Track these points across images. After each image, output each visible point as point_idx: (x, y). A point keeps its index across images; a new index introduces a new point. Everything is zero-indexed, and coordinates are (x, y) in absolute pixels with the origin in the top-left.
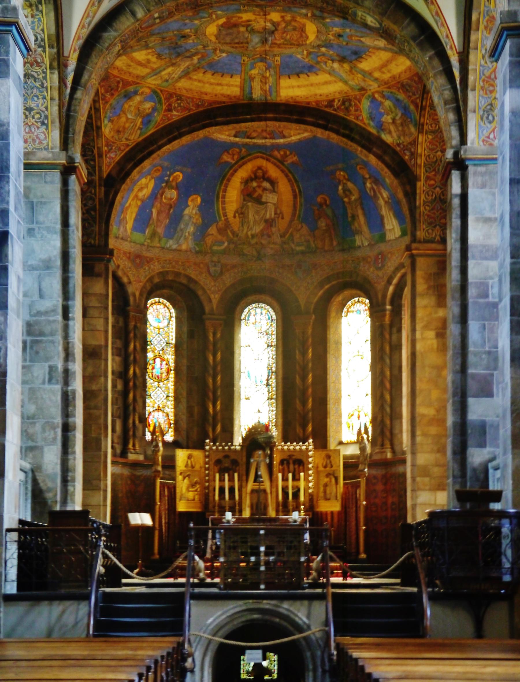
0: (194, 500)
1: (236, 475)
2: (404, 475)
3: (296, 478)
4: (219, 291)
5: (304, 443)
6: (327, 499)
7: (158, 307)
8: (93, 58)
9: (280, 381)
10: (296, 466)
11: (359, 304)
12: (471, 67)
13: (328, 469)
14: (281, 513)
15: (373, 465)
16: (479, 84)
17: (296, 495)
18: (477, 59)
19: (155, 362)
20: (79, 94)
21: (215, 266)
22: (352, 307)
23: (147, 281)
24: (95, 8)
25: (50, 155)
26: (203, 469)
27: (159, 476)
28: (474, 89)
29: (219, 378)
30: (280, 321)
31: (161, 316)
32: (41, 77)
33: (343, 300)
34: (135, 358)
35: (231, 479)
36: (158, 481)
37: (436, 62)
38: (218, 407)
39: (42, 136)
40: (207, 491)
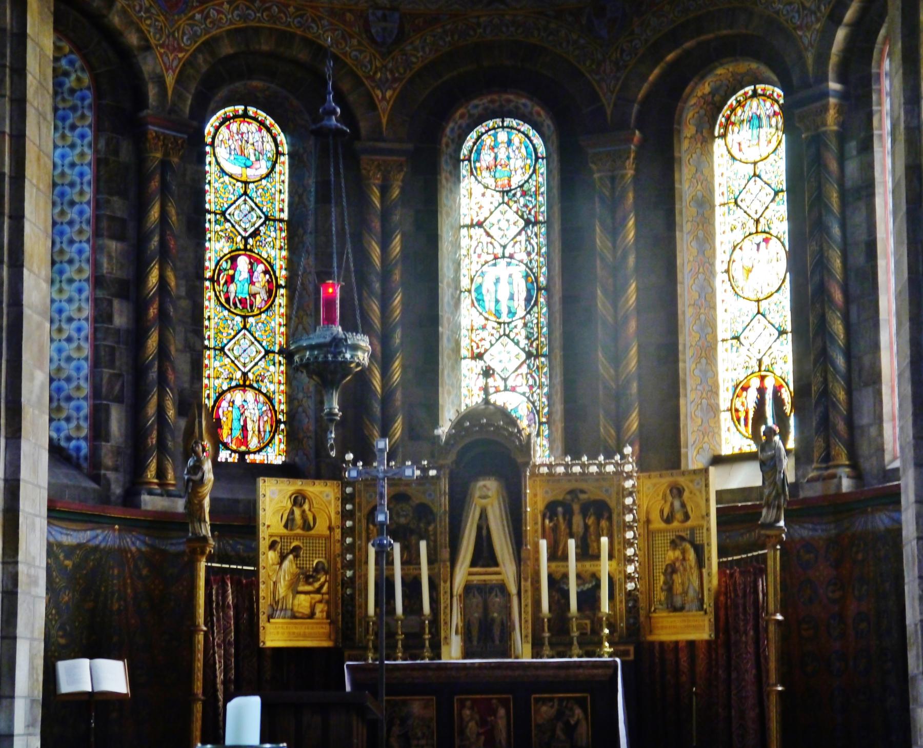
0: (312, 615)
1: (423, 545)
2: (896, 534)
3: (587, 553)
4: (395, 80)
5: (609, 456)
6: (675, 609)
7: (244, 127)
9: (557, 307)
10: (591, 521)
11: (755, 102)
13: (675, 524)
14: (547, 650)
15: (801, 510)
17: (589, 599)
19: (234, 266)
21: (384, 18)
22: (739, 111)
23: (198, 50)
26: (338, 534)
27: (203, 553)
29: (398, 300)
30: (555, 157)
31: (250, 150)
33: (713, 93)
34: (163, 243)
35: (411, 559)
36: (203, 564)
38: (397, 376)
40: (349, 591)
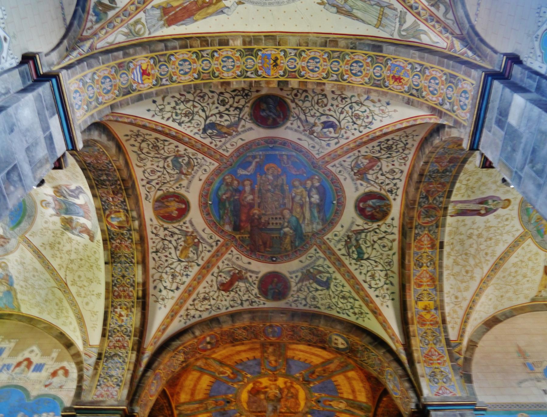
8: (164, 354)
12: (414, 348)
16: (422, 359)
18: (416, 343)
20: (149, 374)
24: (169, 320)
25: (116, 403)
28: (419, 363)
32: (124, 356)
37: (388, 355)
39: (115, 393)
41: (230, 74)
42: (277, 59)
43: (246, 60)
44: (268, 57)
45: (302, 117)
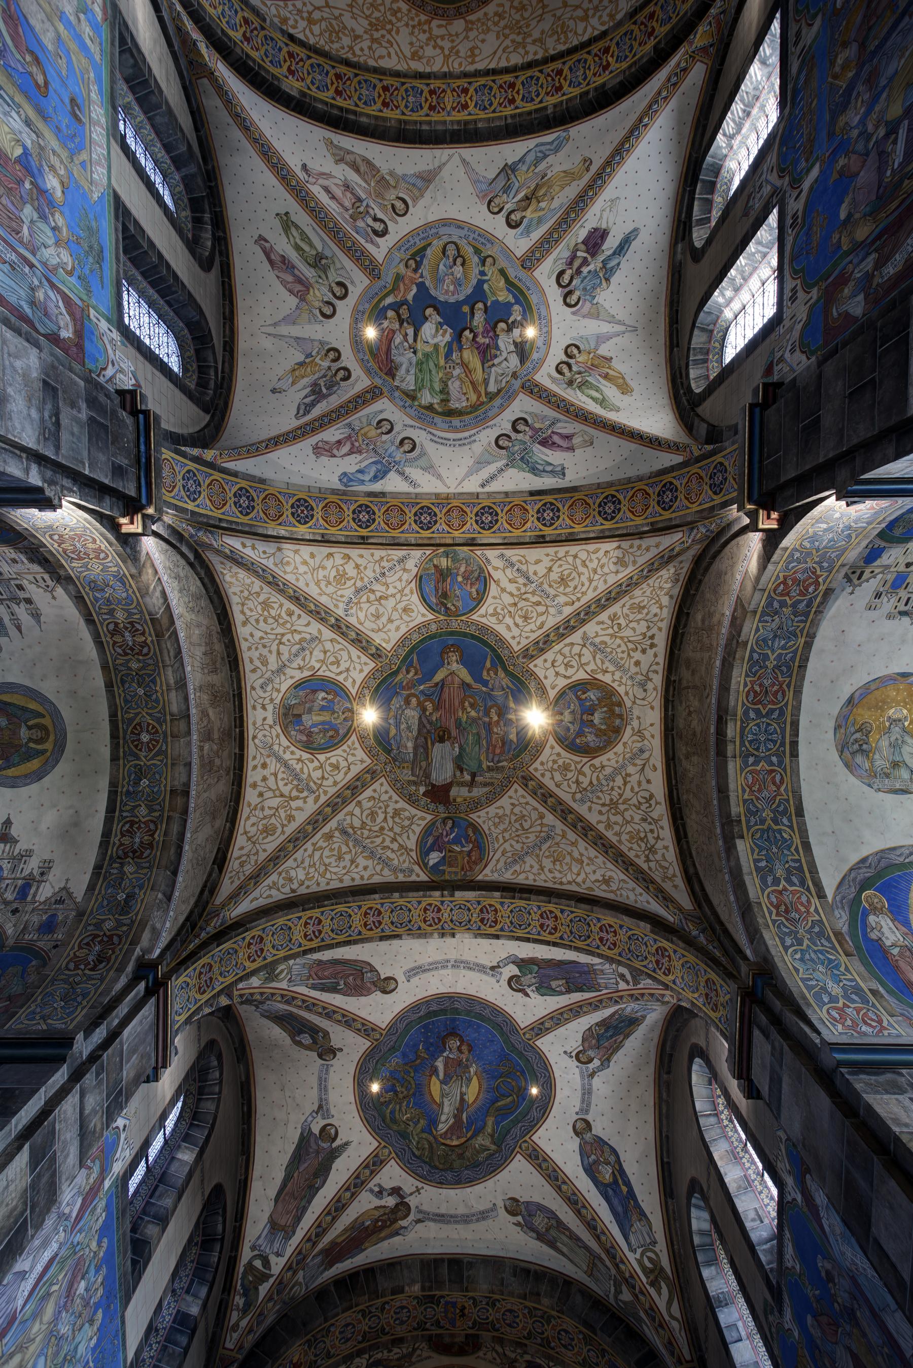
41: (404, 1327)
42: (464, 1308)
43: (425, 1309)
44: (454, 1304)
45: (500, 1350)
